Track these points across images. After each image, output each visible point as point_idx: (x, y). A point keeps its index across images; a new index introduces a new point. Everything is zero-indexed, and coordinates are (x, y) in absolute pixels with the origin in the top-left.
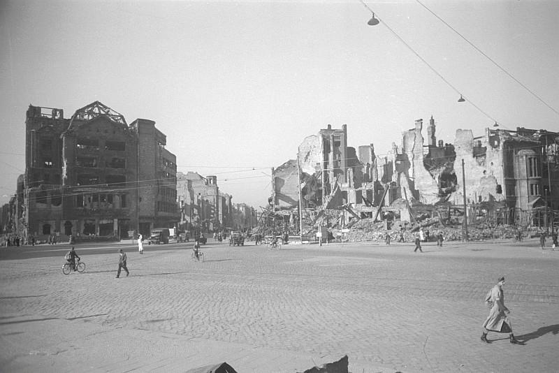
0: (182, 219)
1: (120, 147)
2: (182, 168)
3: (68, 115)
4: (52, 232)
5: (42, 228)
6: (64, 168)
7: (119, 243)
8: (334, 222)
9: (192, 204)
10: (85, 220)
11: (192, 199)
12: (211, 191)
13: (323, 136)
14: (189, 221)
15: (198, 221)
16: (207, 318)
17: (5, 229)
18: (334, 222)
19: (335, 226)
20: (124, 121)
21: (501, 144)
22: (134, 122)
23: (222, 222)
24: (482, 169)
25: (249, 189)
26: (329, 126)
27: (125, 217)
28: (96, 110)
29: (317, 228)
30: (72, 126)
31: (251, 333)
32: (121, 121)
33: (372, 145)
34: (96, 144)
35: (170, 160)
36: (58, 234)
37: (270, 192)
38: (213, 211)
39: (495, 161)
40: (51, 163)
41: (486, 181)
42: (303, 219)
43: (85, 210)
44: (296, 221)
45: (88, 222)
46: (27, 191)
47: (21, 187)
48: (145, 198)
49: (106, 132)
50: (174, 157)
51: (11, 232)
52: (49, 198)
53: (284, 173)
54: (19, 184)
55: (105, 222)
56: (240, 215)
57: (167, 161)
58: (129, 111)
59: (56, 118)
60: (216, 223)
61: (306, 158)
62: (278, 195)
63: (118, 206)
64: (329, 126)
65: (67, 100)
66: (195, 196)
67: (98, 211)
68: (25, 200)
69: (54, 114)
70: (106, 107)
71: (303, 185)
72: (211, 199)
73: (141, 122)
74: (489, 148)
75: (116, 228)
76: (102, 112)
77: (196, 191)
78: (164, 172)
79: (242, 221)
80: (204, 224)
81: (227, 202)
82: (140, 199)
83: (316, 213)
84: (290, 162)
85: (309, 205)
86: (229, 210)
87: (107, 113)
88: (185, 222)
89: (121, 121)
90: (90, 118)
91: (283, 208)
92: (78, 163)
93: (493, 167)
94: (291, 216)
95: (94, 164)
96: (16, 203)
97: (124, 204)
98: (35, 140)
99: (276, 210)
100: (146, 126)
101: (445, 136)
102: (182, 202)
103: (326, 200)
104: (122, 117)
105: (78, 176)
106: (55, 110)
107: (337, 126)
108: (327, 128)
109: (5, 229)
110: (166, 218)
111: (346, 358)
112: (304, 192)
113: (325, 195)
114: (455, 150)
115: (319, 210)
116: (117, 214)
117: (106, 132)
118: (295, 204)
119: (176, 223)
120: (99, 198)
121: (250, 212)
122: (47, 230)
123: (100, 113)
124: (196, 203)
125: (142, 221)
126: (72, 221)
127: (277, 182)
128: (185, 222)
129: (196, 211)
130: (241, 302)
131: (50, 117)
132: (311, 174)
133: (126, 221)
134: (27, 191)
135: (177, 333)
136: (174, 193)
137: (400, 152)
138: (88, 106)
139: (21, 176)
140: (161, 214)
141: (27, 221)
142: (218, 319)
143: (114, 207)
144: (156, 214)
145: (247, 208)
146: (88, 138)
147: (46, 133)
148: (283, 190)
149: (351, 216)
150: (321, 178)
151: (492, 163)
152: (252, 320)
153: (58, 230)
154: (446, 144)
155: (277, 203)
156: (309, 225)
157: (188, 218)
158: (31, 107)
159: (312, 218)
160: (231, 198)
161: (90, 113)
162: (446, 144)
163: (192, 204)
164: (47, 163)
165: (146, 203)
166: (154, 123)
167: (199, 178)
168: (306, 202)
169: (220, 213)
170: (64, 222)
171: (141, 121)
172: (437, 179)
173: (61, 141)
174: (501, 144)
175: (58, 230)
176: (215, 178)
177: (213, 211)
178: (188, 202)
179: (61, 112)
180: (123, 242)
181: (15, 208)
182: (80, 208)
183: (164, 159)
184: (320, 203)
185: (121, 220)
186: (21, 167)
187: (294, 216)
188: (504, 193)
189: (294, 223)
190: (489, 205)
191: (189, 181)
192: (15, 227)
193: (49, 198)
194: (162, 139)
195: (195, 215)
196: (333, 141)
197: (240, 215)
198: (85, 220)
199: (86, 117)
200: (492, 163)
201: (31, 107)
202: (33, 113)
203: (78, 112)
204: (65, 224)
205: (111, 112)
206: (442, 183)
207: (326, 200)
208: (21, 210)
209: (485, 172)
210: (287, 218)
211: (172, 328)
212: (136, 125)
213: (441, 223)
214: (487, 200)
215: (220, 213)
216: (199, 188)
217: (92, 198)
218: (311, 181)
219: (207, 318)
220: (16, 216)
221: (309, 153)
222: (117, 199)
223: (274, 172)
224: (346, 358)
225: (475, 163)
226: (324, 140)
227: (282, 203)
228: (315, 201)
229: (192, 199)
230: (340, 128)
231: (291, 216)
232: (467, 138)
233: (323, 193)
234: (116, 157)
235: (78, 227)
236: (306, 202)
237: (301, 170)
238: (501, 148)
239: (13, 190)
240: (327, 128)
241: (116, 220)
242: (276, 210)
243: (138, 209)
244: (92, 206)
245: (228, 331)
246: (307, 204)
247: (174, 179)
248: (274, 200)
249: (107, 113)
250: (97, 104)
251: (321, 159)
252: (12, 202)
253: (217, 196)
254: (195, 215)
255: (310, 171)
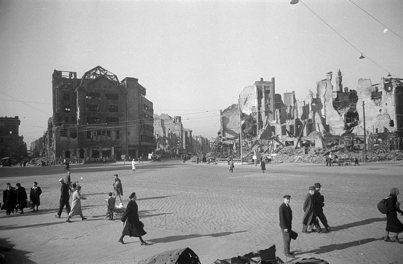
0: (158, 147)
1: (114, 97)
2: (157, 111)
3: (79, 76)
4: (71, 156)
5: (64, 152)
6: (78, 113)
7: (115, 164)
8: (265, 148)
9: (165, 137)
10: (93, 148)
11: (164, 133)
12: (177, 127)
13: (257, 86)
14: (162, 149)
15: (169, 148)
16: (175, 217)
17: (41, 155)
18: (265, 148)
19: (266, 151)
20: (117, 79)
21: (394, 89)
22: (124, 80)
23: (185, 148)
24: (378, 108)
25: (203, 124)
26: (262, 79)
27: (119, 146)
28: (98, 72)
29: (253, 153)
30: (83, 84)
31: (206, 227)
32: (115, 80)
33: (294, 92)
34: (98, 95)
35: (149, 106)
36: (75, 158)
37: (219, 127)
38: (179, 142)
39: (389, 102)
40: (69, 110)
41: (381, 117)
42: (243, 146)
43: (92, 141)
44: (238, 148)
45: (95, 149)
46: (54, 128)
47: (50, 126)
48: (132, 133)
49: (105, 87)
50: (152, 104)
51: (45, 156)
52: (68, 133)
53: (229, 114)
54: (49, 124)
55: (105, 149)
56: (198, 144)
57: (147, 107)
58: (120, 72)
59: (72, 78)
60: (181, 150)
61: (245, 102)
62: (225, 129)
63: (114, 139)
64: (262, 79)
65: (78, 65)
66: (167, 131)
67: (100, 142)
68: (53, 135)
69: (71, 76)
70: (105, 70)
71: (243, 122)
72: (178, 133)
73: (129, 80)
74: (384, 92)
75: (113, 153)
76: (102, 74)
77: (167, 127)
78: (145, 114)
79: (200, 148)
80: (173, 151)
81: (189, 135)
82: (129, 133)
83: (252, 142)
84: (233, 106)
85: (247, 136)
86: (190, 141)
87: (106, 74)
88: (160, 149)
89: (115, 80)
90: (94, 78)
91: (228, 139)
92: (87, 109)
94: (235, 144)
95: (98, 109)
96: (48, 136)
97: (118, 137)
98: (58, 94)
99: (224, 140)
100: (132, 81)
101: (350, 84)
102: (158, 135)
103: (260, 133)
104: (116, 76)
105: (88, 118)
106: (71, 73)
107: (268, 79)
108: (260, 80)
109: (41, 155)
110: (146, 147)
111: (274, 246)
112: (243, 127)
113: (259, 129)
114: (357, 95)
115: (254, 140)
116: (113, 144)
117: (105, 87)
118: (238, 136)
119: (154, 150)
120: (102, 133)
121: (205, 142)
122: (68, 155)
123: (101, 74)
124: (167, 136)
125: (130, 148)
126: (83, 149)
127: (224, 121)
128: (160, 149)
129: (167, 141)
130: (199, 206)
131: (68, 78)
132: (249, 114)
133: (120, 149)
134: (54, 128)
135: (155, 226)
136: (151, 129)
137: (315, 97)
138: (93, 70)
139: (50, 118)
140: (144, 143)
141: (55, 149)
142: (183, 217)
143: (111, 138)
144: (140, 143)
145: (202, 139)
147: (66, 90)
148: (228, 126)
149: (278, 144)
150: (256, 117)
152: (207, 218)
153: (75, 155)
154: (351, 90)
155: (224, 135)
156: (248, 151)
157: (161, 146)
158: (55, 71)
159: (250, 145)
160: (191, 132)
161: (95, 74)
162: (351, 90)
163: (165, 137)
164: (67, 109)
165: (133, 135)
166: (137, 80)
167: (169, 118)
168: (245, 134)
169: (184, 142)
170: (79, 149)
171: (128, 79)
172: (343, 117)
173: (75, 94)
174: (394, 89)
175: (75, 155)
176: (180, 118)
177: (179, 142)
178: (162, 135)
179: (75, 74)
180: (118, 163)
181: (47, 140)
182: (89, 140)
183: (144, 105)
184: (255, 135)
185: (119, 148)
186: (49, 112)
187: (236, 144)
188: (395, 126)
189: (237, 149)
190: (384, 135)
191: (162, 120)
192: (47, 153)
193: (68, 133)
194: (143, 91)
195: (166, 144)
196: (264, 90)
197: (198, 144)
198: (93, 148)
199: (92, 77)
201: (55, 71)
202: (57, 75)
203: (86, 74)
204: (79, 151)
205: (108, 73)
206: (347, 120)
207: (260, 133)
208: (51, 141)
209: (380, 110)
210: (231, 146)
211: (152, 223)
212: (125, 82)
213: (346, 149)
214: (383, 131)
215: (184, 142)
216: (169, 125)
217: (97, 133)
218: (249, 119)
219: (175, 217)
220: (48, 146)
221: (247, 99)
222: (114, 134)
223: (222, 113)
224: (274, 246)
225: (373, 104)
226: (258, 89)
227: (228, 135)
228: (251, 134)
229: (164, 133)
230: (270, 80)
231: (235, 144)
232: (367, 84)
233: (258, 127)
234: (112, 104)
235: (88, 153)
236: (245, 134)
237: (241, 111)
238: (393, 92)
239: (45, 128)
240: (260, 80)
241: (113, 148)
242: (224, 140)
243: (127, 140)
244: (97, 139)
245: (190, 225)
246: (245, 136)
247: (151, 119)
248: (221, 133)
249: (106, 74)
250: (98, 68)
251: (256, 103)
252: (45, 136)
253: (182, 131)
254: (166, 144)
255: (248, 112)
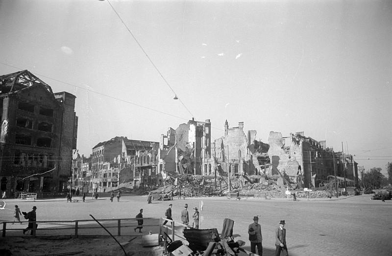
1: (46, 112)
24: (287, 155)
26: (193, 118)
41: (291, 163)
64: (193, 118)
93: (296, 155)
104: (50, 88)
107: (201, 119)
108: (192, 119)
146: (28, 101)
151: (295, 153)
166: (75, 97)
185: (48, 177)
188: (302, 170)
200: (295, 153)
209: (290, 157)
238: (301, 145)
240: (192, 119)
250: (26, 73)
